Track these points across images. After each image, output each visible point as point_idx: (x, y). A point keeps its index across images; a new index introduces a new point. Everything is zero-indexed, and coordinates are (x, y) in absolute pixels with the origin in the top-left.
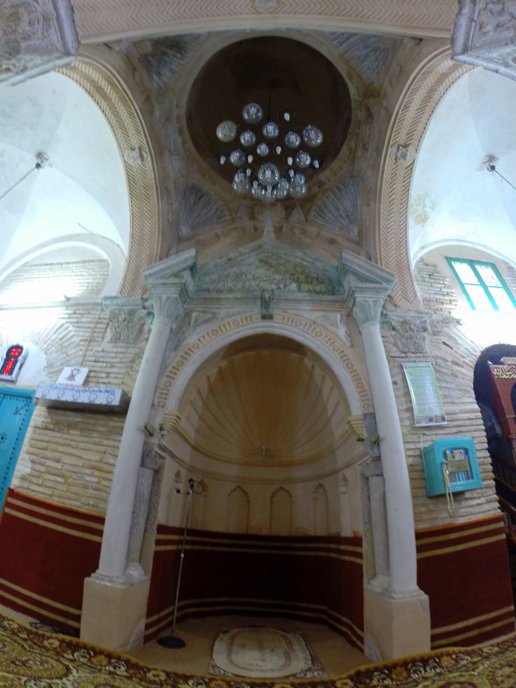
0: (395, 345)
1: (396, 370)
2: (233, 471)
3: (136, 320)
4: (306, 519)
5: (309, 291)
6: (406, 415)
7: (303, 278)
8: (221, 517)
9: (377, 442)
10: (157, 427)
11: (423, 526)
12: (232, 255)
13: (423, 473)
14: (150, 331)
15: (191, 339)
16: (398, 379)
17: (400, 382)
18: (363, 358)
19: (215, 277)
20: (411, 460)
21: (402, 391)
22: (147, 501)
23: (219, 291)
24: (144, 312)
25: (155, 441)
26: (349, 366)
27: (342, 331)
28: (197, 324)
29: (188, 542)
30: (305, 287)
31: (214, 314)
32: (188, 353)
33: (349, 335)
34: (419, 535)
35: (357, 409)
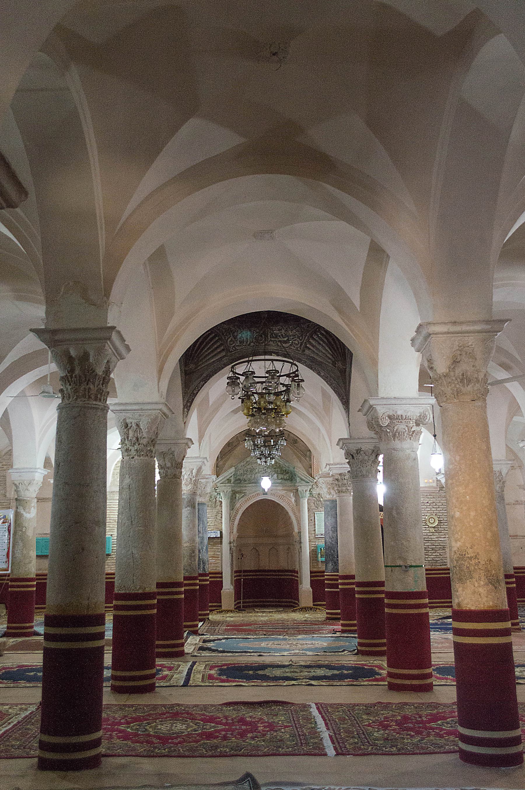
0: (314, 503)
1: (312, 515)
2: (251, 541)
3: (213, 497)
4: (283, 565)
5: (282, 479)
6: (314, 532)
7: (279, 470)
8: (250, 565)
9: (301, 543)
10: (232, 541)
11: (315, 570)
12: (248, 460)
13: (314, 553)
14: (221, 502)
15: (238, 505)
16: (313, 518)
17: (313, 520)
18: (299, 511)
19: (242, 472)
20: (313, 548)
21: (313, 523)
22: (232, 564)
23: (245, 481)
24: (216, 493)
25: (232, 545)
26: (294, 514)
27: (293, 500)
28: (239, 499)
29: (244, 576)
30: (281, 476)
31: (245, 493)
32: (238, 511)
33: (296, 501)
34: (311, 572)
35: (296, 530)
